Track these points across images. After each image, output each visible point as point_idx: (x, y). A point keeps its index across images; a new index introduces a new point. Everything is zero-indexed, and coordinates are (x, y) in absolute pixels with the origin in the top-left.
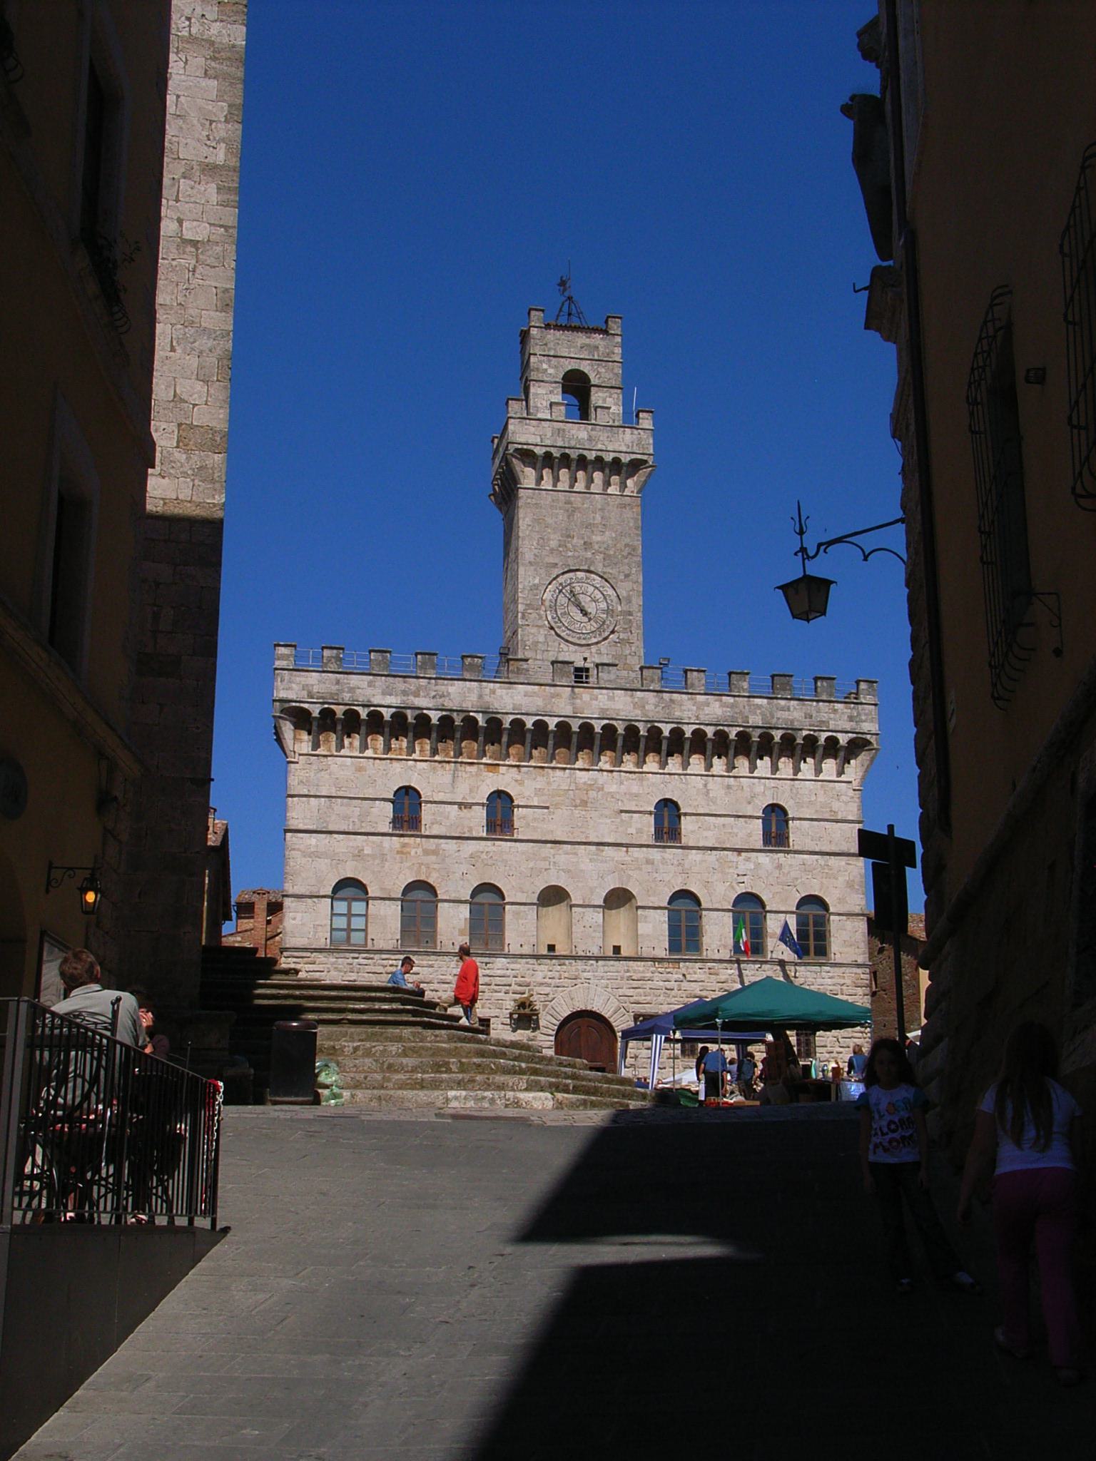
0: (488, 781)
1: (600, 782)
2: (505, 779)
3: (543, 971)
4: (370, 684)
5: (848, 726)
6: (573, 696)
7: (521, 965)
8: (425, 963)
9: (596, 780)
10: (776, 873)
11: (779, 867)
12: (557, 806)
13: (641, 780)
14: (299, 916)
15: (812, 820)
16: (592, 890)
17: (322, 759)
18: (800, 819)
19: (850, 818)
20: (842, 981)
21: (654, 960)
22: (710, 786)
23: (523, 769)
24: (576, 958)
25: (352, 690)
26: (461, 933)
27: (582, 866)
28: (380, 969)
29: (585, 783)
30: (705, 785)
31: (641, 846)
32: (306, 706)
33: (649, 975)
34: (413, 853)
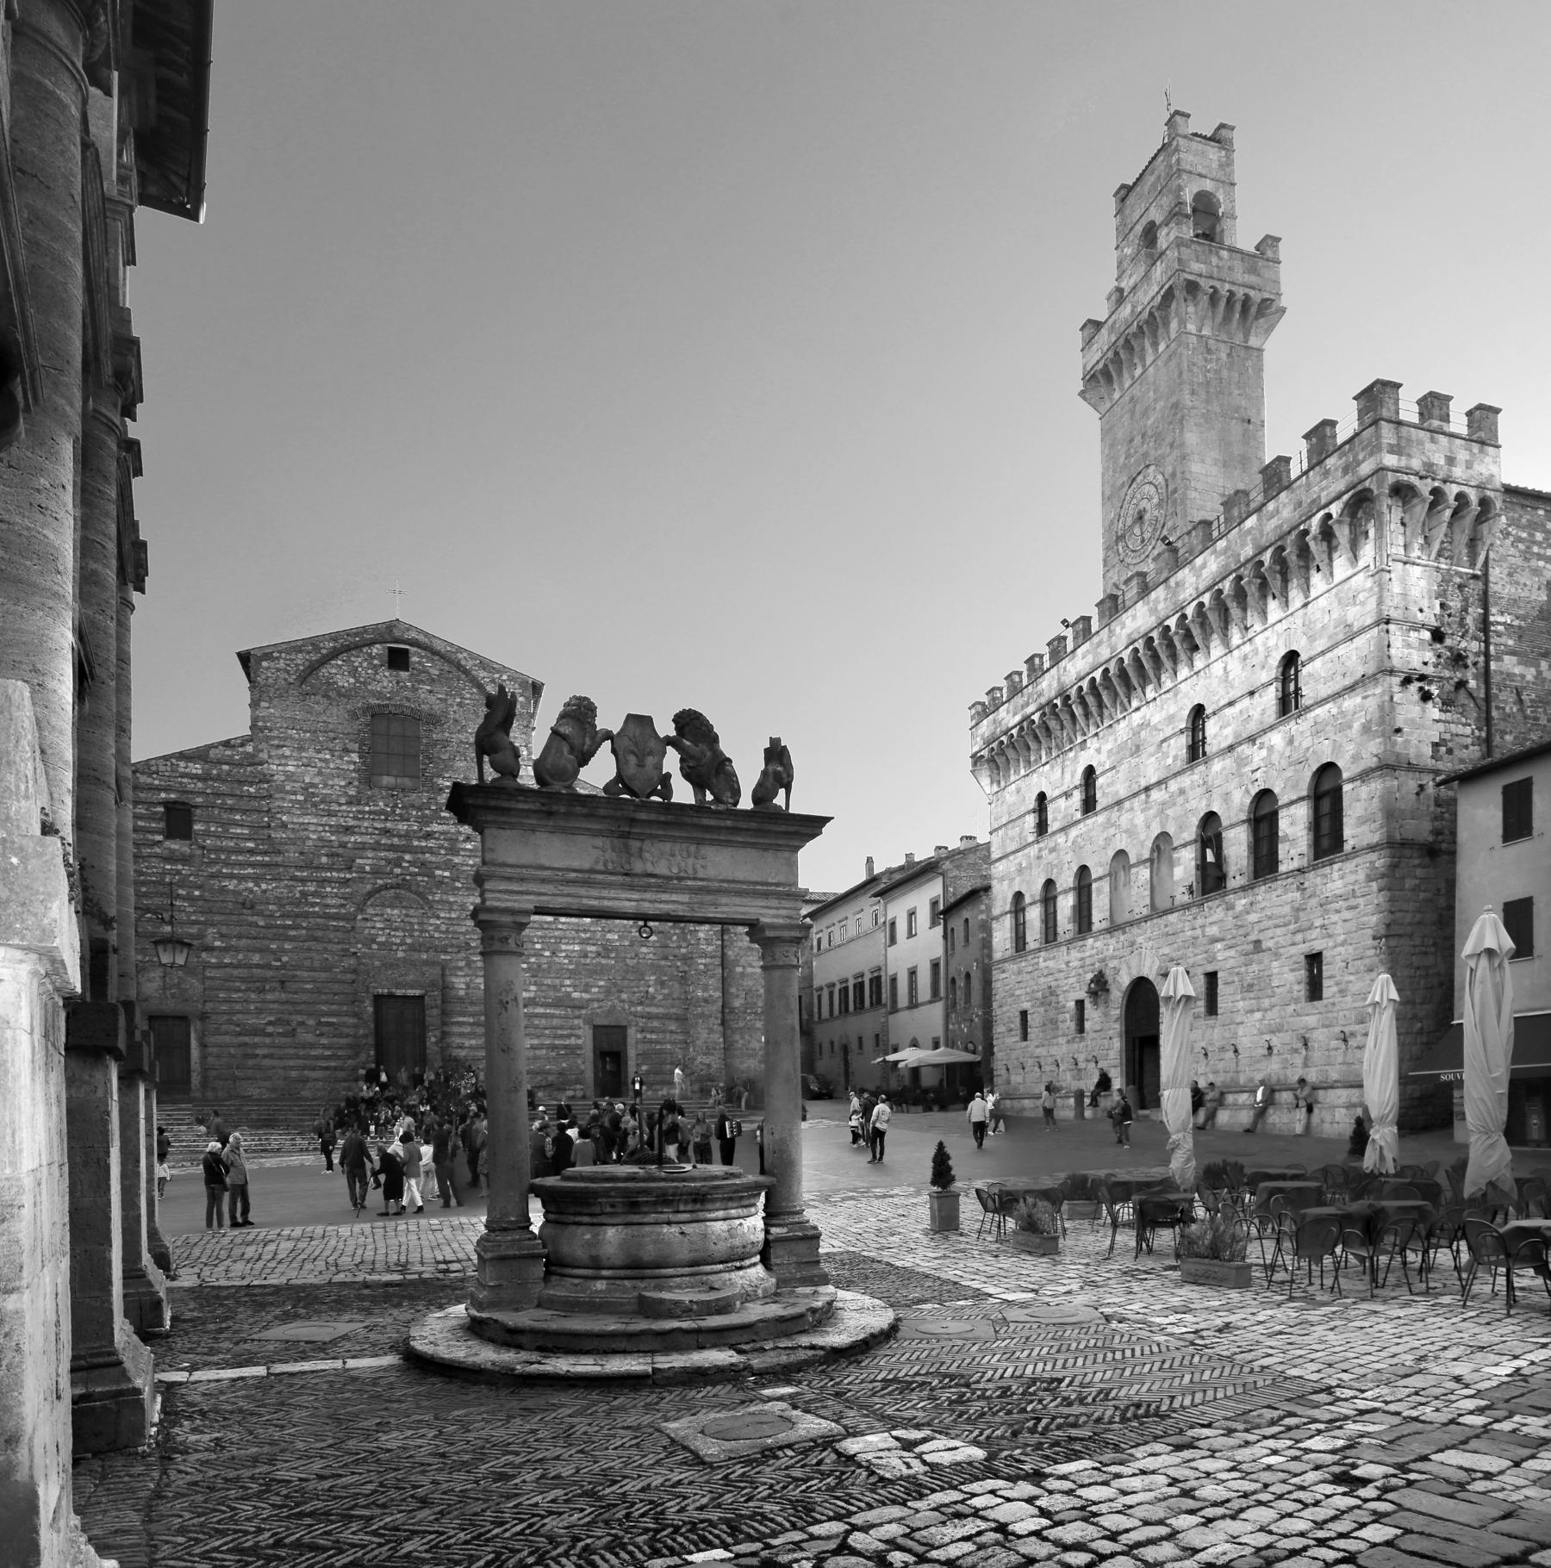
13: (1176, 695)
20: (1352, 878)
21: (1186, 907)
24: (1131, 924)
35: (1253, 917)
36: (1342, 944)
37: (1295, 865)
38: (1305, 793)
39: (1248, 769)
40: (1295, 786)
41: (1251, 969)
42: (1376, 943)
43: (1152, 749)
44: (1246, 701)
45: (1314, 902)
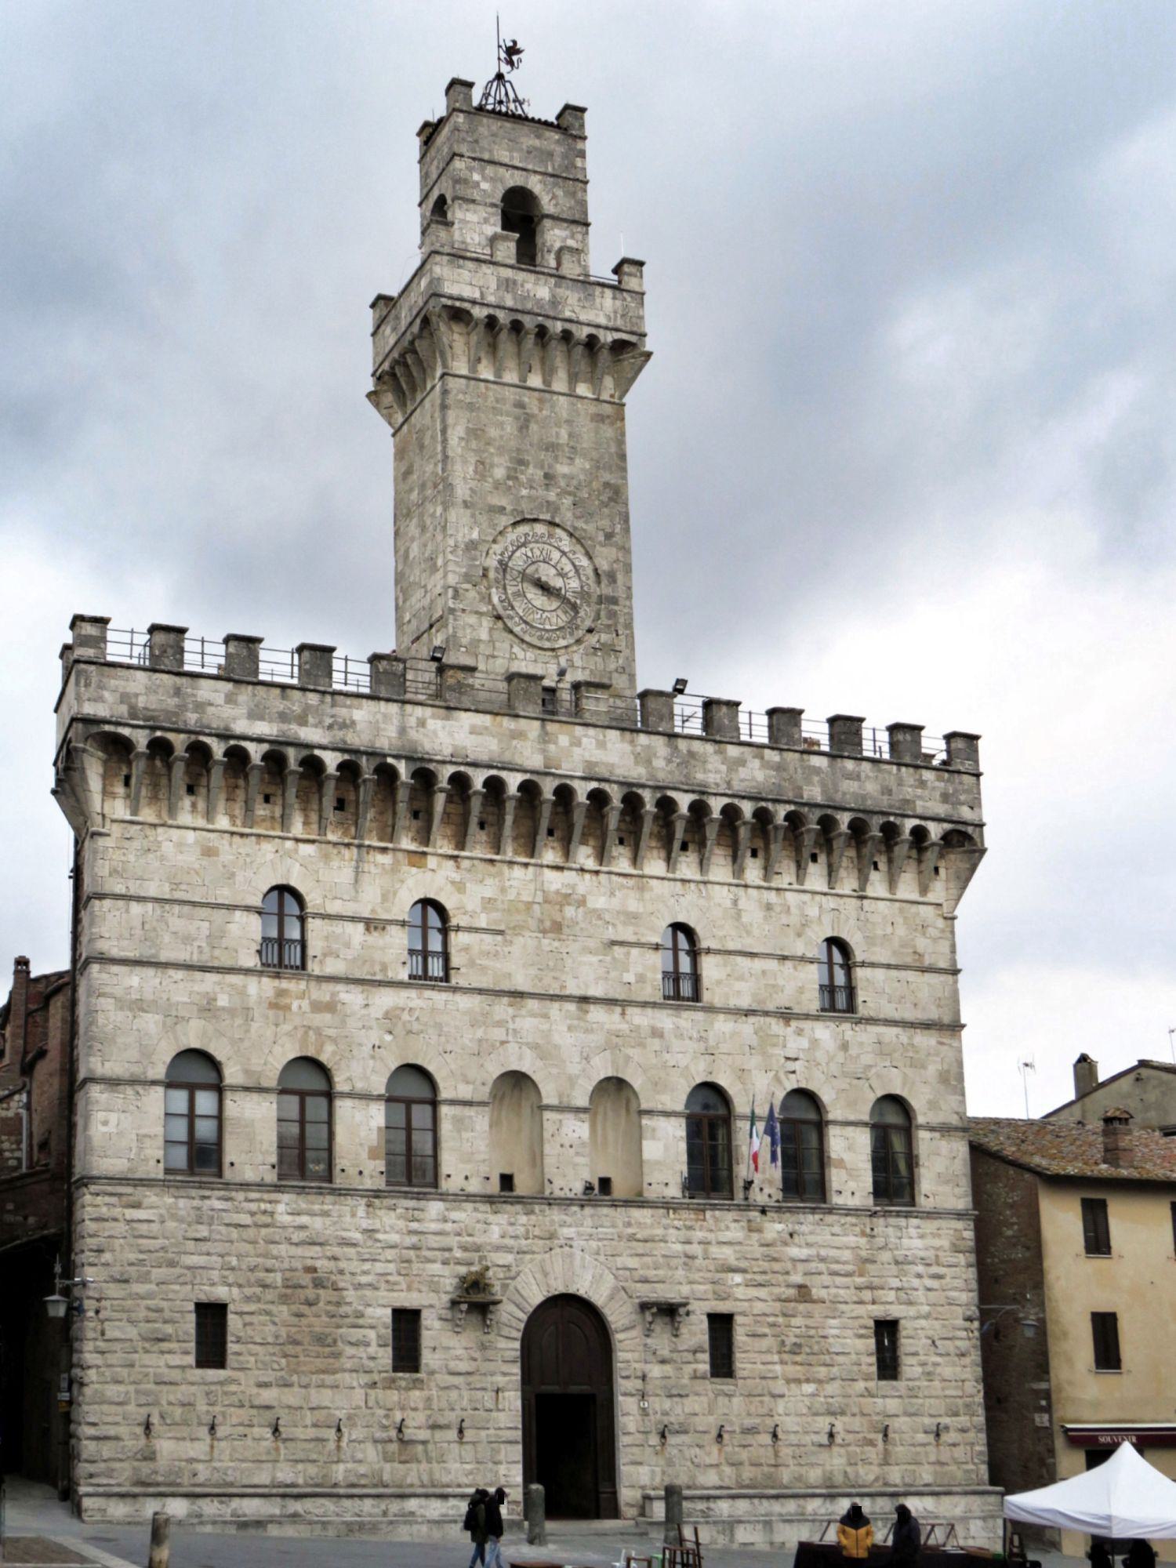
0: (410, 882)
1: (581, 889)
2: (437, 877)
3: (497, 1227)
4: (230, 699)
7: (464, 1215)
8: (316, 1207)
9: (573, 887)
10: (840, 1057)
12: (518, 929)
13: (642, 889)
14: (113, 1117)
15: (888, 966)
16: (572, 1080)
17: (149, 831)
18: (873, 965)
19: (943, 964)
20: (937, 1242)
21: (667, 1205)
22: (742, 904)
23: (465, 864)
24: (550, 1202)
25: (200, 707)
26: (373, 1155)
27: (557, 1039)
28: (246, 1219)
29: (557, 892)
30: (735, 902)
31: (645, 1004)
32: (126, 731)
33: (659, 1232)
34: (295, 1007)
35: (794, 1252)
36: (927, 1317)
38: (866, 1118)
39: (778, 1051)
40: (852, 1104)
41: (795, 1322)
43: (592, 943)
44: (772, 965)
45: (886, 1256)
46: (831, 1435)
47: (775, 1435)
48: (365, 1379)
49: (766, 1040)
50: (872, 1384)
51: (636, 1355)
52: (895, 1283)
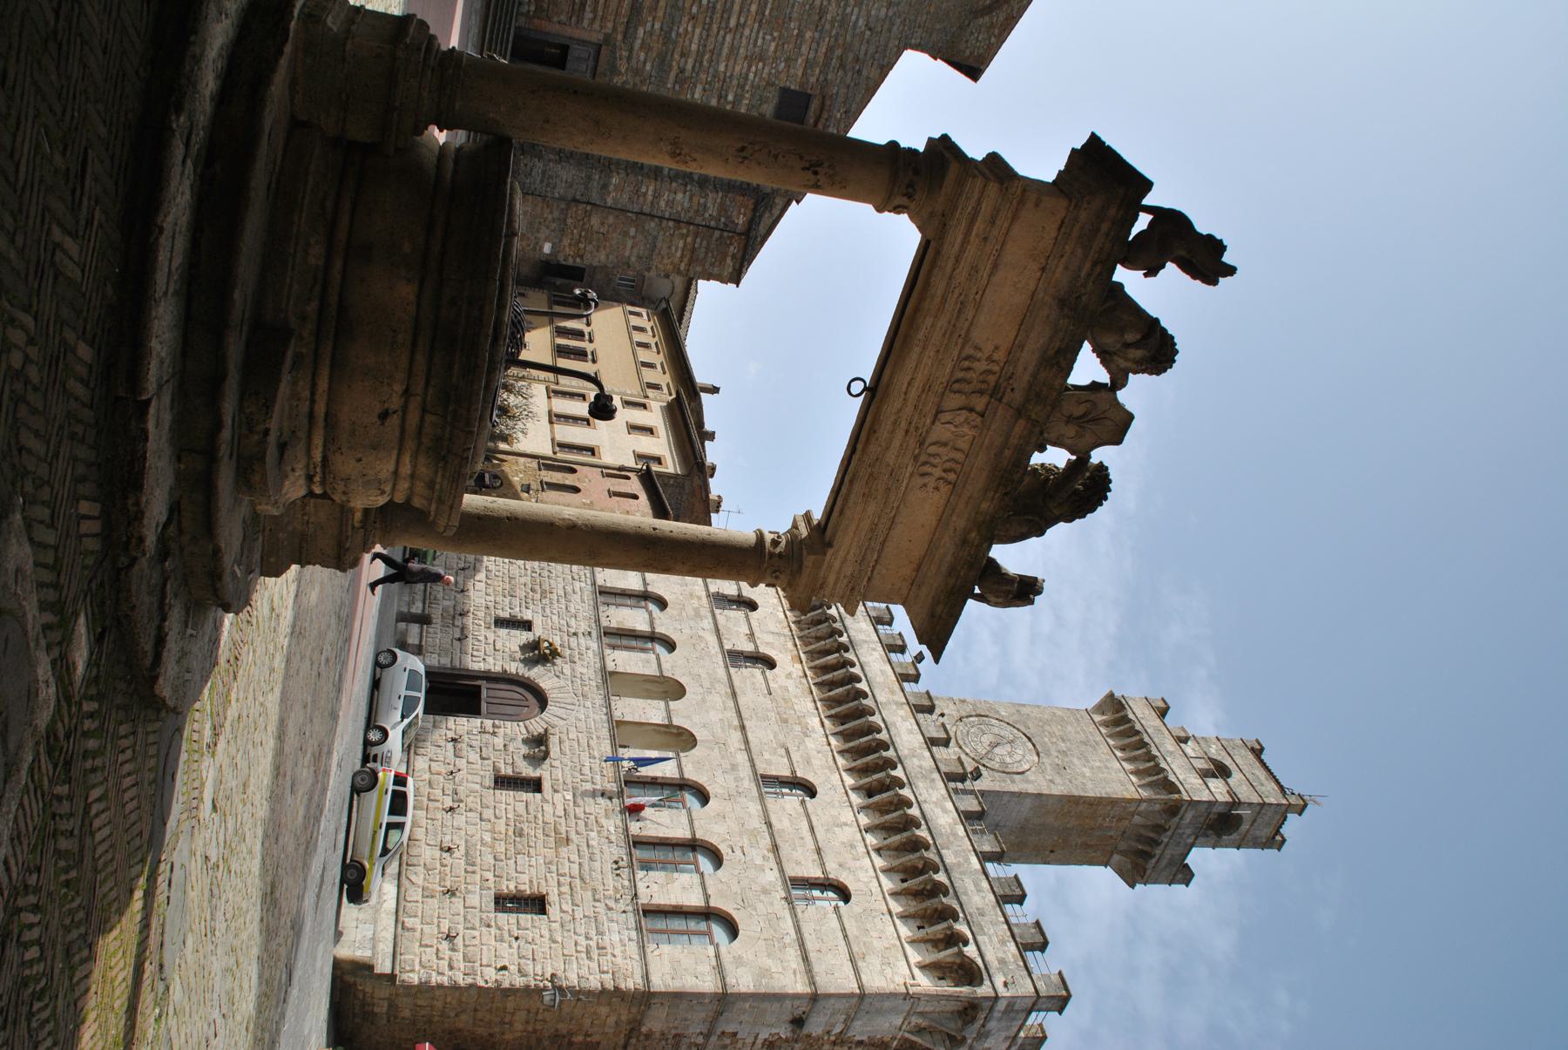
5: (991, 957)
6: (899, 704)
7: (591, 658)
11: (765, 891)
15: (844, 930)
16: (688, 717)
31: (751, 760)
37: (641, 886)
39: (746, 841)
42: (548, 976)
43: (781, 737)
45: (601, 908)
46: (450, 849)
47: (451, 809)
48: (491, 605)
49: (754, 834)
50: (491, 884)
51: (508, 731)
52: (579, 914)
